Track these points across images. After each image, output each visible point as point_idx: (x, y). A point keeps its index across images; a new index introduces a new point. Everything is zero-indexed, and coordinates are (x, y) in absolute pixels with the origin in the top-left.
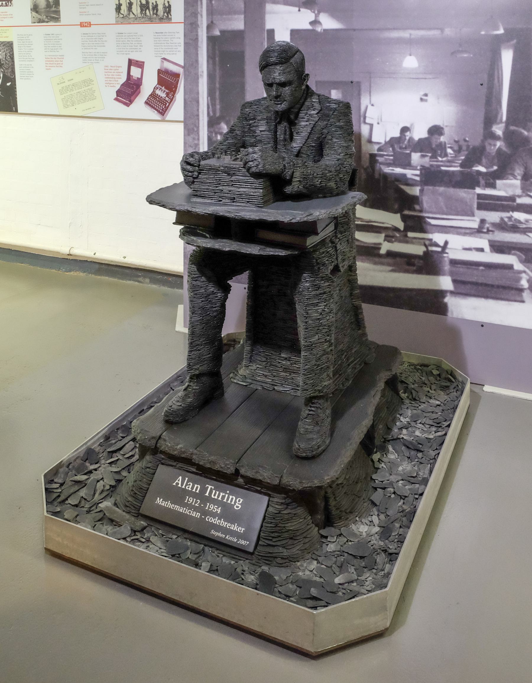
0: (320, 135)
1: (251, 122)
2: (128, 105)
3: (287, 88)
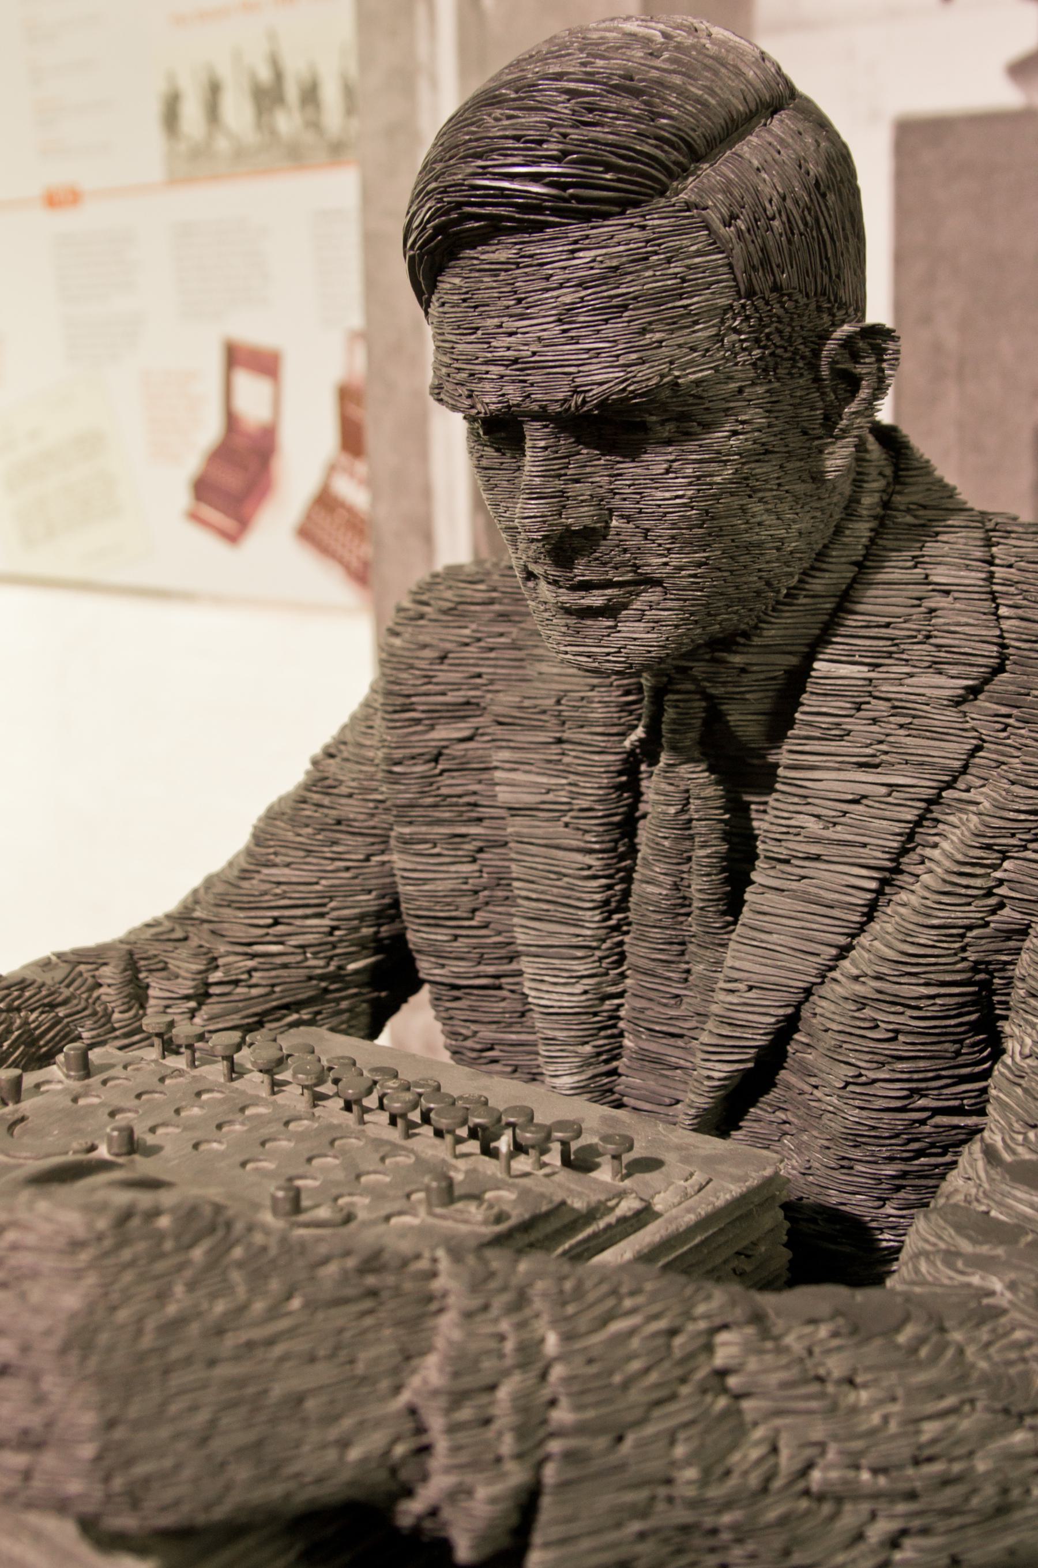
0: (973, 913)
1: (443, 733)
2: (232, 538)
3: (656, 460)
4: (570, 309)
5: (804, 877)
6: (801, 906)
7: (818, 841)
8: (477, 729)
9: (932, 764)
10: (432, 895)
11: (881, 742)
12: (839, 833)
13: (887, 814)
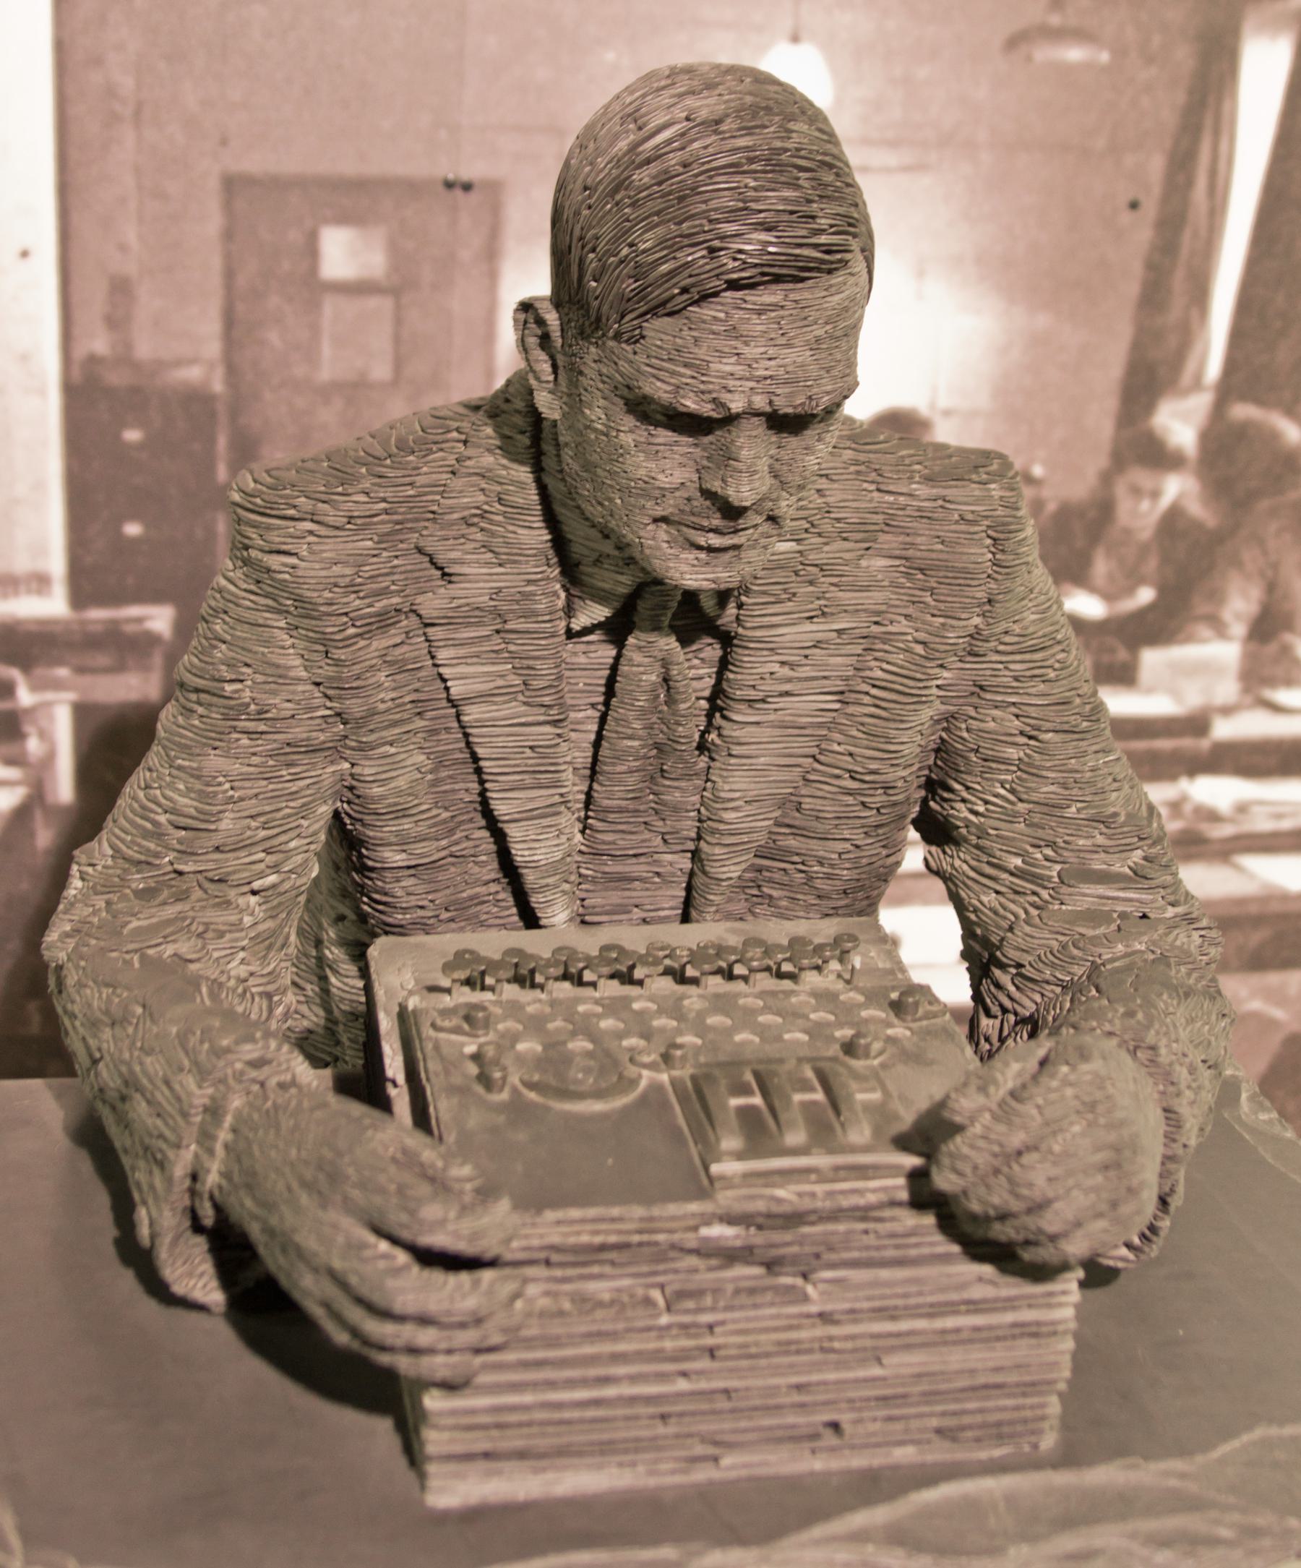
4: (818, 340)
5: (776, 710)
6: (778, 732)
7: (789, 680)
8: (407, 633)
9: (865, 610)
10: (400, 793)
11: (818, 598)
12: (805, 672)
13: (843, 652)
